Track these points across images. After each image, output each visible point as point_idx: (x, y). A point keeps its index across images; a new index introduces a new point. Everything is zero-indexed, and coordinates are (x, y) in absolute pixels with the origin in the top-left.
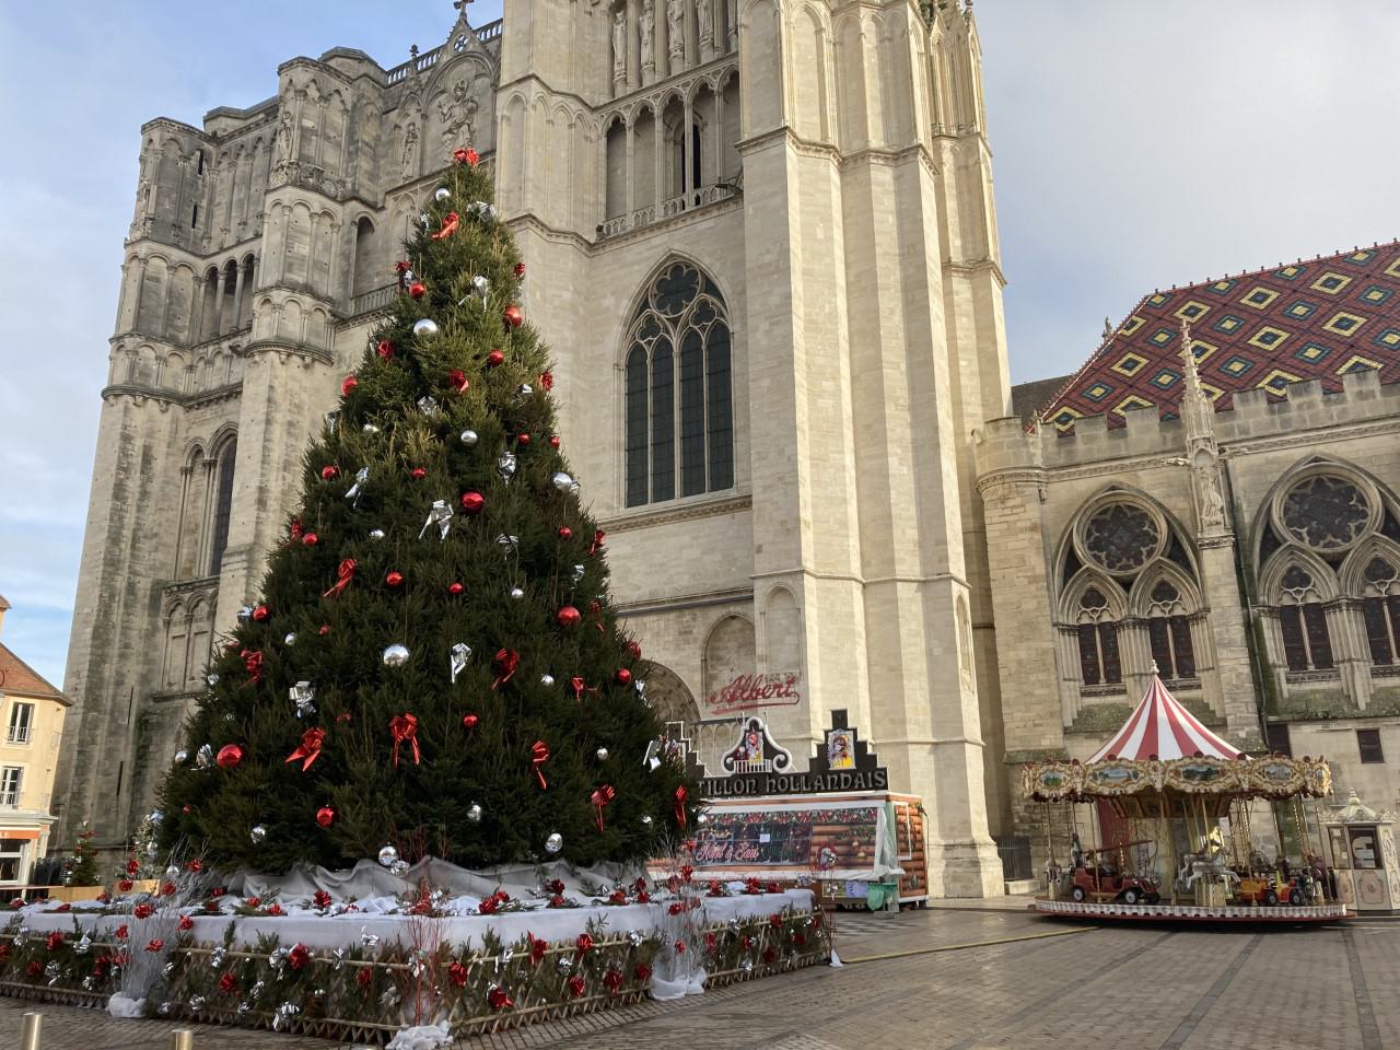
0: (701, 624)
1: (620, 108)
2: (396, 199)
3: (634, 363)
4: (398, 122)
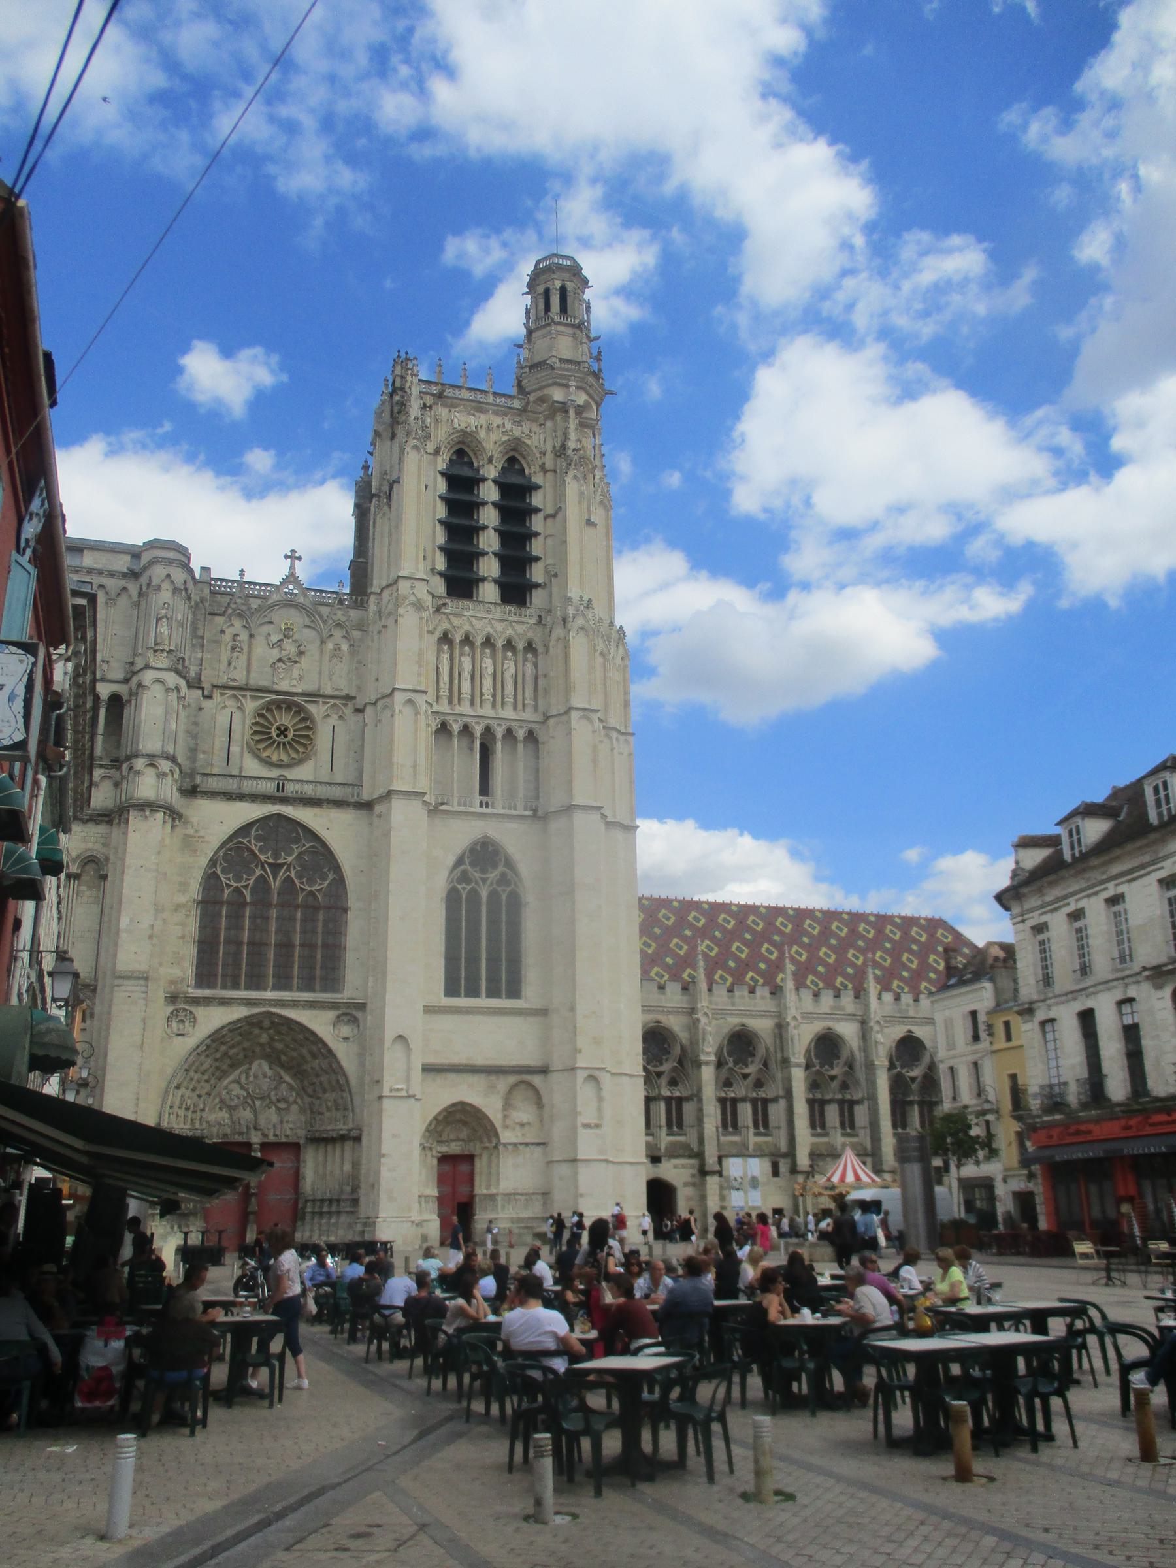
0: (504, 1083)
1: (450, 719)
2: (222, 694)
3: (452, 899)
4: (224, 628)
